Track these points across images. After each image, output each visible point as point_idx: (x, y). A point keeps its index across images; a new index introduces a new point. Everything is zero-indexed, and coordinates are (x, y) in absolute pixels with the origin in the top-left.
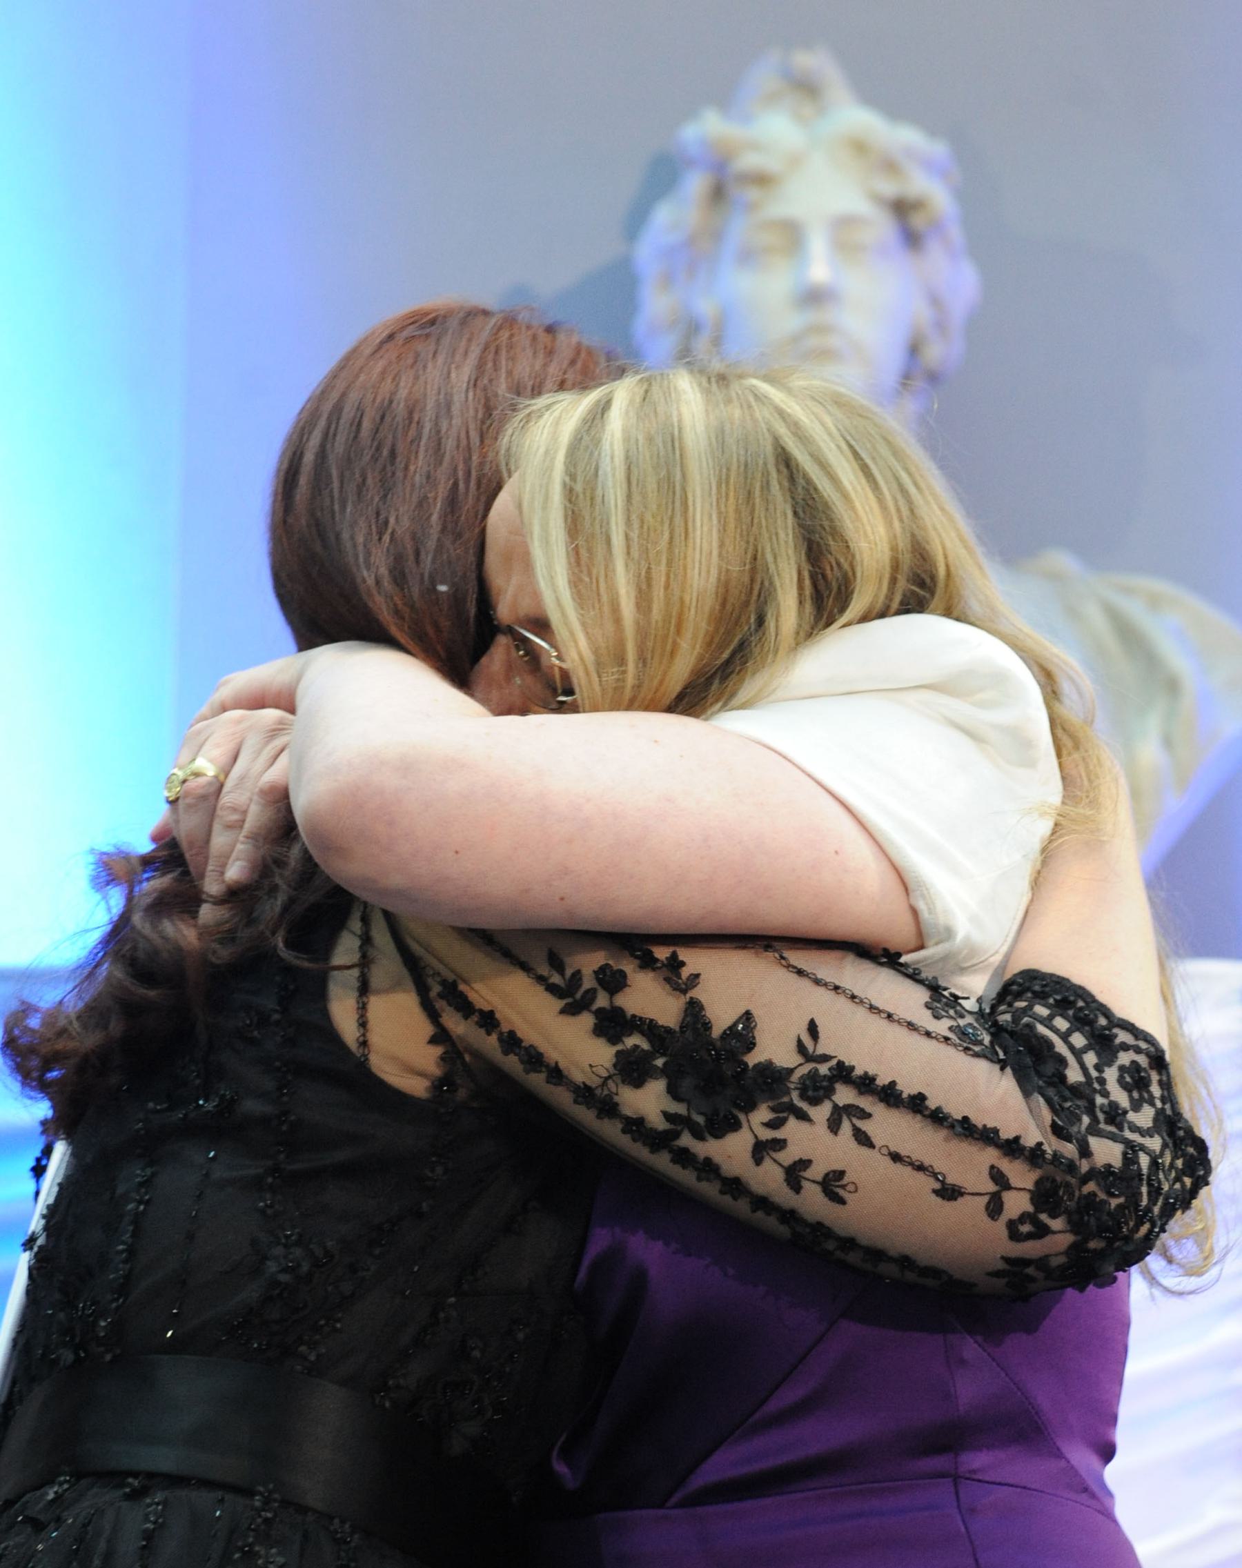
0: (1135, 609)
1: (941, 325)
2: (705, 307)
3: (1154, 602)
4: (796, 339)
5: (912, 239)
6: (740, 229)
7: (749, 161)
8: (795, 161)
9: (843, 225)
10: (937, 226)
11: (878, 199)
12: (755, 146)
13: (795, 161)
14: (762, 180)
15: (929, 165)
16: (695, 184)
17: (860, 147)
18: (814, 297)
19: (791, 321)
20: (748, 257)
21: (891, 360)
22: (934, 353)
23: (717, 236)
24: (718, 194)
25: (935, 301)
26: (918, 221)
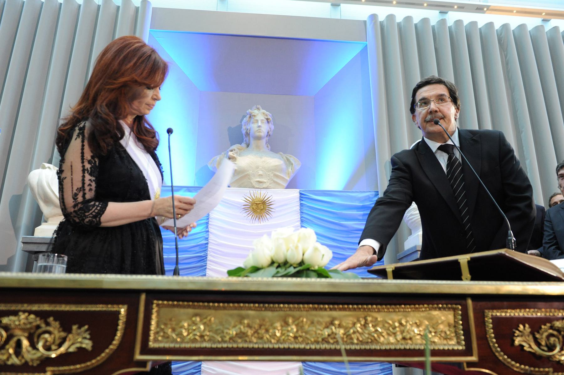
0: (288, 157)
1: (270, 130)
2: (249, 128)
3: (290, 157)
4: (257, 130)
5: (268, 122)
6: (252, 120)
7: (253, 114)
8: (258, 114)
9: (262, 120)
10: (271, 121)
11: (265, 118)
12: (254, 113)
13: (258, 114)
14: (254, 116)
15: (270, 116)
16: (248, 116)
17: (264, 113)
18: (259, 126)
19: (257, 129)
20: (253, 123)
21: (267, 133)
22: (270, 133)
23: (250, 121)
24: (250, 117)
25: (270, 128)
26: (269, 120)
